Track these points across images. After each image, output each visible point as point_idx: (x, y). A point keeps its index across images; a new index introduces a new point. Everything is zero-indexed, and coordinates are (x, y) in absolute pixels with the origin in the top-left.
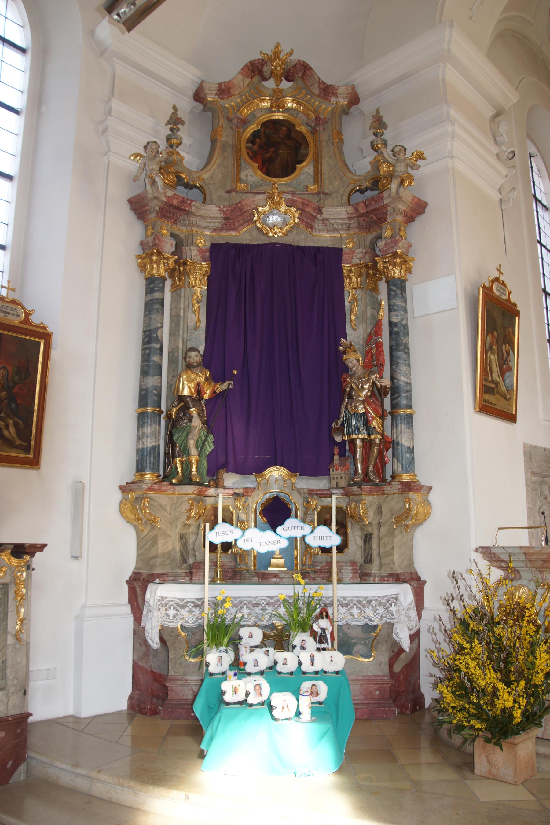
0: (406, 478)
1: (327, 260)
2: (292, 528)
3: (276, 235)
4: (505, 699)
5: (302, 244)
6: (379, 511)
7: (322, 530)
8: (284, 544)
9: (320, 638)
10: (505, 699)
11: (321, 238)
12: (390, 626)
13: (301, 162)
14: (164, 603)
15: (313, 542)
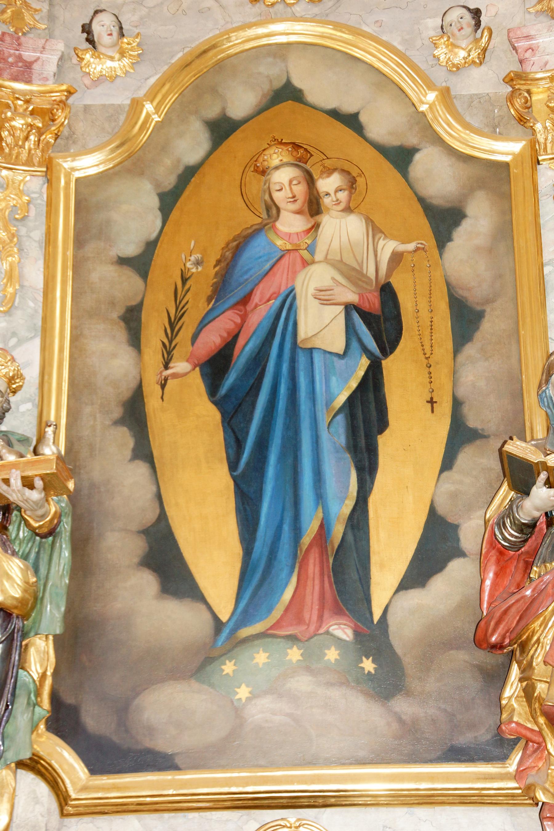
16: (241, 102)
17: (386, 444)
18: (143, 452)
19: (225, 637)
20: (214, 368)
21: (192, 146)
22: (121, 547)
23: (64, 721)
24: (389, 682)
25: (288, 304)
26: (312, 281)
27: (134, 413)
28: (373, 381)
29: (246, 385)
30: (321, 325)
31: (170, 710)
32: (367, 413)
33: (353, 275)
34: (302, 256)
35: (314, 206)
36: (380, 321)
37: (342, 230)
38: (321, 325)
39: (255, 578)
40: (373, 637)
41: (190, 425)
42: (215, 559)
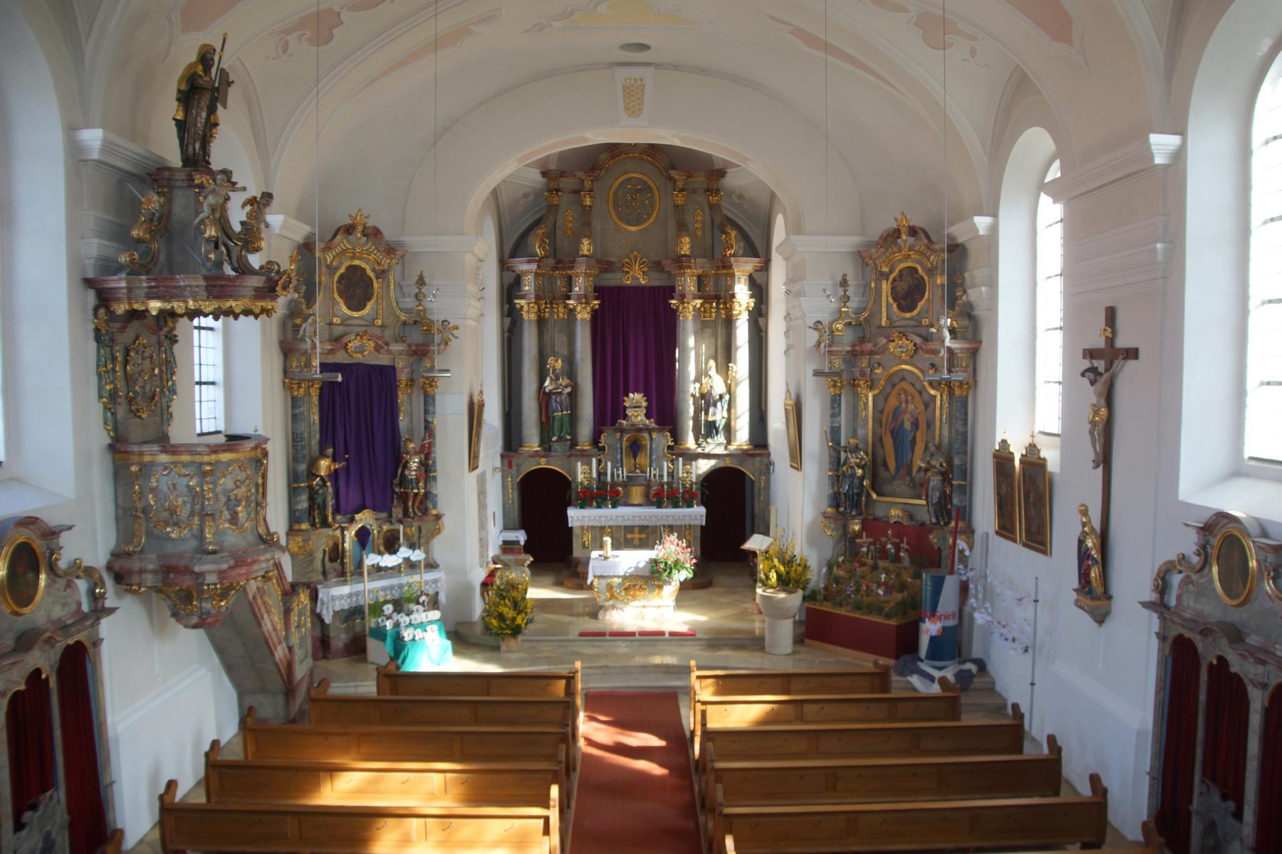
0: (434, 512)
1: (387, 374)
2: (404, 552)
3: (358, 358)
4: (519, 621)
5: (372, 363)
6: (420, 529)
7: (417, 551)
8: (401, 561)
9: (423, 604)
10: (519, 621)
11: (383, 360)
12: (437, 593)
13: (369, 300)
14: (333, 598)
15: (413, 558)
16: (896, 380)
17: (916, 448)
18: (882, 446)
19: (893, 478)
20: (892, 432)
21: (889, 389)
22: (879, 461)
23: (873, 489)
24: (914, 487)
25: (903, 422)
26: (907, 416)
27: (881, 440)
28: (914, 437)
29: (897, 434)
30: (908, 425)
31: (887, 488)
32: (913, 442)
33: (912, 415)
34: (905, 412)
35: (907, 402)
36: (916, 425)
37: (911, 407)
38: (908, 425)
39: (897, 468)
40: (912, 480)
41: (888, 441)
42: (892, 464)
